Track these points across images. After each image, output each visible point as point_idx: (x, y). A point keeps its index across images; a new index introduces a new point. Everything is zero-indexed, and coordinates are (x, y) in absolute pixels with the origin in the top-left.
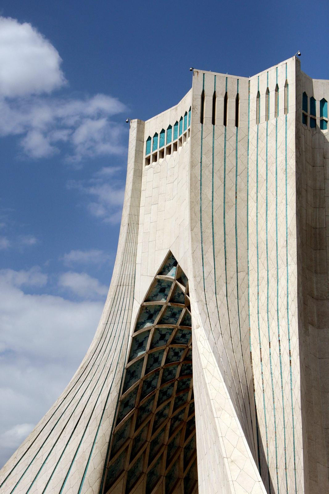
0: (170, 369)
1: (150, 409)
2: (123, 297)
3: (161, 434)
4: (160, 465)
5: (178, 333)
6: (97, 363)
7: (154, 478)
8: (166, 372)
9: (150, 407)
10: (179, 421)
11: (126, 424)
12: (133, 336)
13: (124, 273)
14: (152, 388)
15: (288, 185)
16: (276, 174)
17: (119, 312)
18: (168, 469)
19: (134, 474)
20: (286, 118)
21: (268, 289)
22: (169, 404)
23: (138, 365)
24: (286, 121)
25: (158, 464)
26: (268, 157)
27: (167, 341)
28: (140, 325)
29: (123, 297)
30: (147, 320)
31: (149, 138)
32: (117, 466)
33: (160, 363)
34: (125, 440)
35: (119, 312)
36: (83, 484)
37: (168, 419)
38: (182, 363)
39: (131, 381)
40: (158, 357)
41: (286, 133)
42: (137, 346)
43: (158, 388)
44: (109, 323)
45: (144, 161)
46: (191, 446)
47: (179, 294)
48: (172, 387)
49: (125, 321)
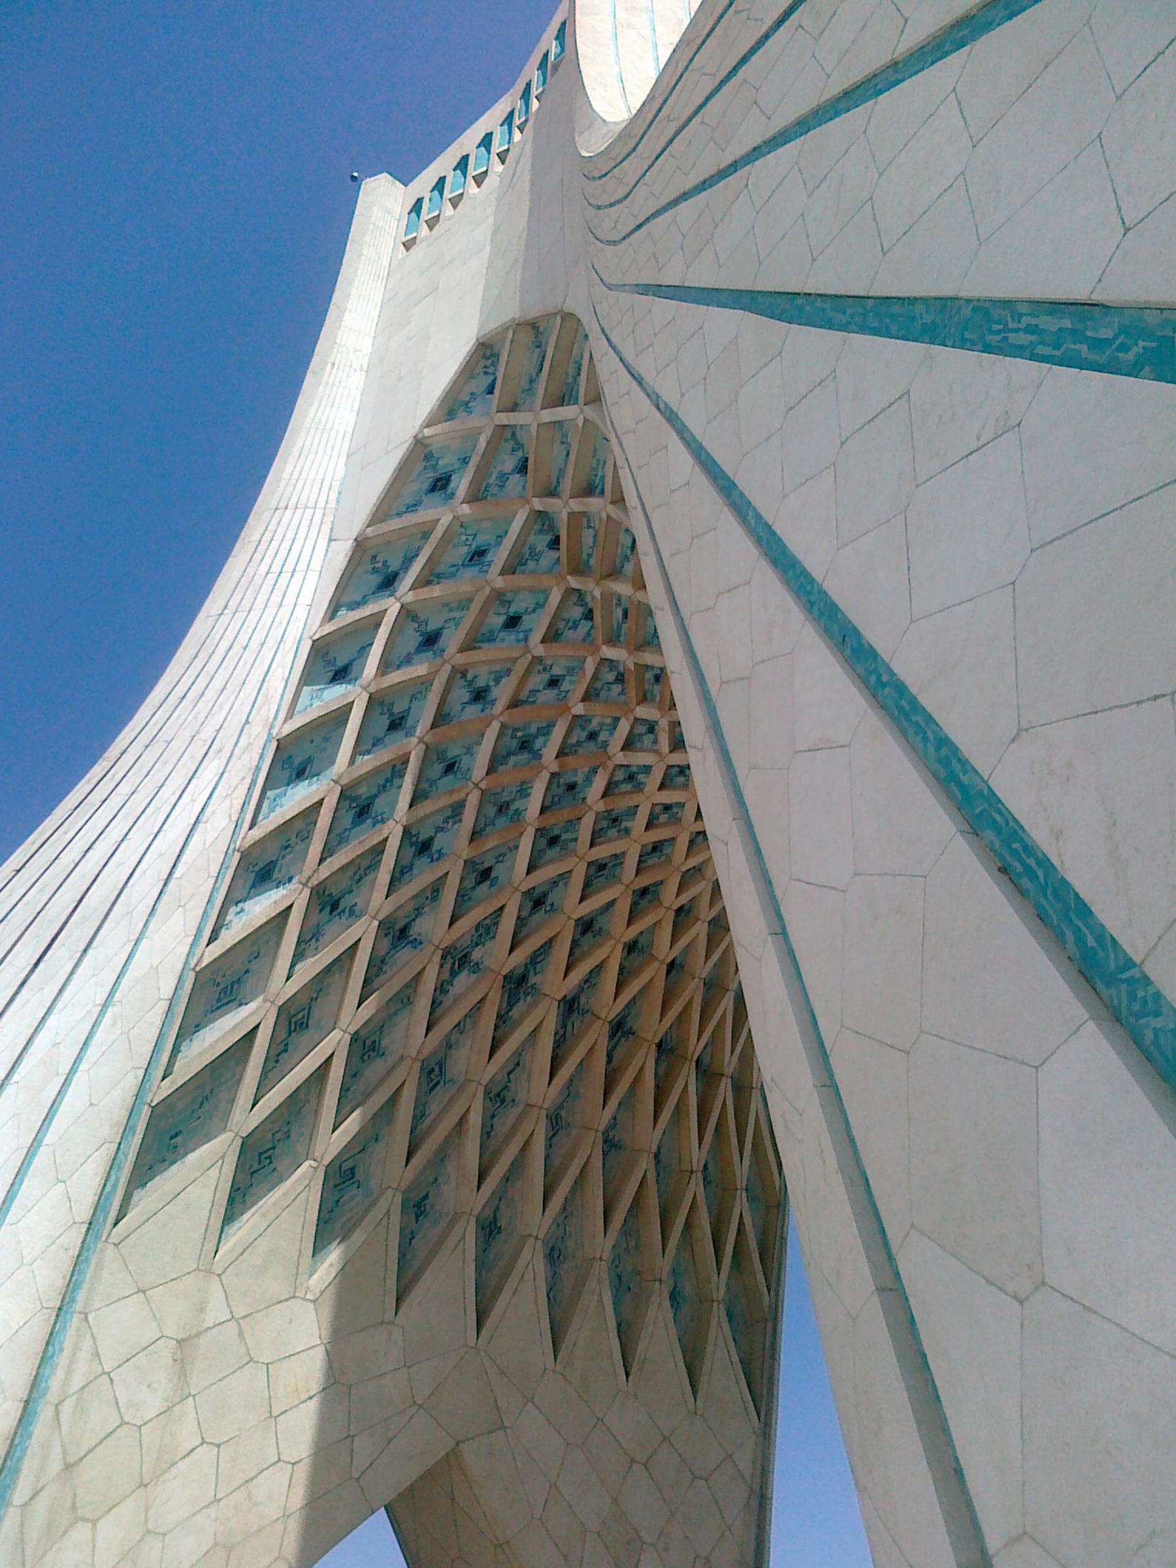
0: (451, 754)
1: (358, 907)
5: (491, 613)
7: (352, 1198)
8: (436, 765)
9: (358, 898)
10: (474, 972)
13: (303, 476)
17: (272, 577)
19: (271, 1163)
22: (436, 890)
23: (326, 739)
25: (377, 1140)
32: (196, 1114)
37: (431, 948)
40: (410, 708)
46: (513, 1089)
48: (454, 823)
49: (289, 600)
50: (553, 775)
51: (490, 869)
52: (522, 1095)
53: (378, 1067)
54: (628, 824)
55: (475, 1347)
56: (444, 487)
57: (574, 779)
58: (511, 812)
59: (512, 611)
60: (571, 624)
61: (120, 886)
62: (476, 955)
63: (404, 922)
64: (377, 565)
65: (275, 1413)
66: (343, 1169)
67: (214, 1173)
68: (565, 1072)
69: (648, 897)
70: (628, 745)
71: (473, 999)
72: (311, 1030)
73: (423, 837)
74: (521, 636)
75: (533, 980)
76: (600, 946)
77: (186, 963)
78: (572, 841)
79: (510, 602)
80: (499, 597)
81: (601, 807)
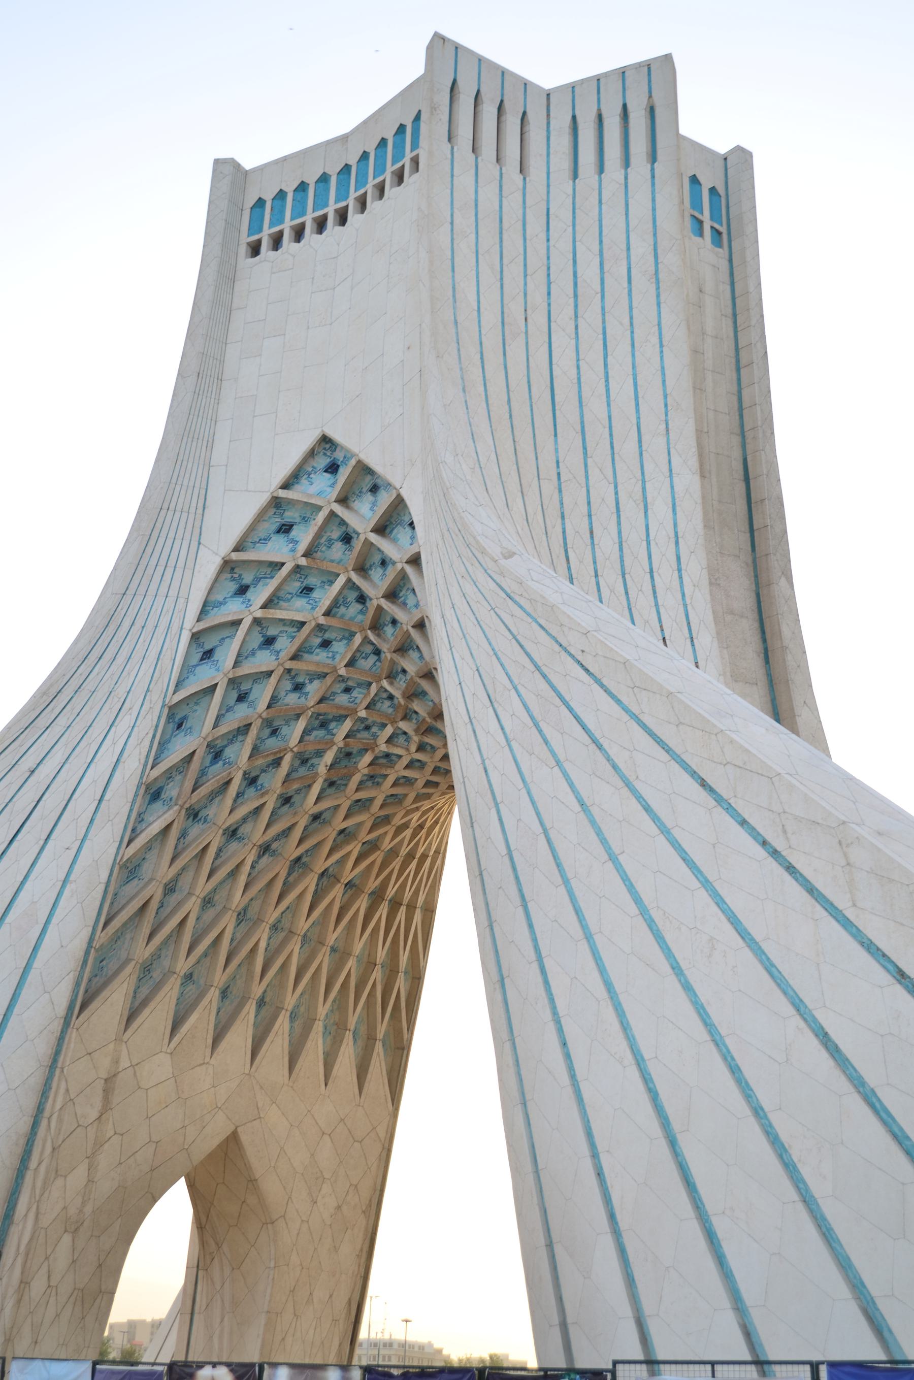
0: (276, 724)
1: (209, 817)
2: (171, 535)
4: (208, 959)
6: (89, 686)
9: (211, 812)
11: (148, 847)
12: (194, 630)
14: (224, 764)
15: (662, 305)
16: (630, 282)
17: (160, 569)
18: (228, 970)
20: (653, 169)
21: (619, 523)
22: (257, 811)
24: (653, 177)
26: (605, 247)
27: (278, 652)
29: (171, 535)
30: (231, 597)
31: (260, 203)
33: (252, 705)
34: (141, 885)
35: (160, 569)
36: (26, 985)
39: (173, 740)
40: (251, 689)
41: (654, 200)
42: (199, 655)
44: (131, 592)
45: (243, 249)
47: (330, 540)
49: (173, 593)
50: (340, 750)
51: (291, 797)
53: (211, 913)
54: (380, 780)
55: (248, 1074)
58: (309, 765)
59: (327, 636)
61: (67, 798)
62: (274, 846)
64: (235, 575)
65: (150, 1115)
67: (125, 985)
68: (316, 913)
70: (389, 741)
71: (271, 876)
72: (176, 893)
73: (253, 774)
74: (330, 655)
75: (304, 859)
76: (348, 844)
77: (115, 860)
80: (320, 628)
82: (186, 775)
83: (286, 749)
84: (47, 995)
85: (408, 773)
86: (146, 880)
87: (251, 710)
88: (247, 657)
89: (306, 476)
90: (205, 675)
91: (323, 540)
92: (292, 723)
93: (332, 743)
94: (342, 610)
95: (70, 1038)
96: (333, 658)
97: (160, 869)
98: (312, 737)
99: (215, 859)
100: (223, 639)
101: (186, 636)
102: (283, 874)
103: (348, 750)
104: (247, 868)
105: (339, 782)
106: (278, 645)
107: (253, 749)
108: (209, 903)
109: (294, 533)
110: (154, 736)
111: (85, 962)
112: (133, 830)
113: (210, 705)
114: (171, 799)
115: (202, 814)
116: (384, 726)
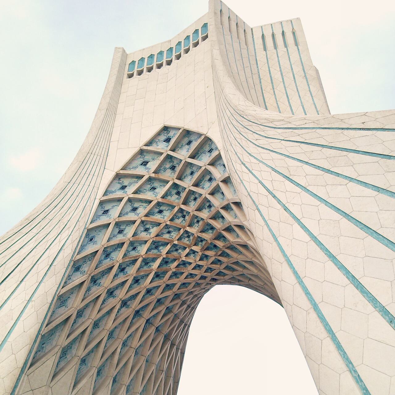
0: (135, 245)
1: (101, 284)
3: (104, 316)
4: (93, 354)
5: (154, 207)
7: (84, 368)
10: (127, 308)
22: (124, 283)
27: (139, 214)
28: (109, 193)
30: (118, 190)
34: (66, 310)
37: (119, 299)
38: (153, 239)
43: (120, 259)
46: (128, 342)
51: (139, 280)
52: (129, 344)
53: (97, 331)
54: (179, 276)
56: (145, 165)
57: (168, 260)
60: (178, 217)
62: (129, 303)
63: (113, 290)
66: (83, 359)
69: (177, 296)
70: (186, 256)
73: (123, 267)
75: (141, 312)
77: (56, 293)
78: (163, 277)
79: (161, 206)
81: (174, 270)
82: (92, 262)
83: (140, 256)
84: (14, 355)
85: (194, 272)
86: (69, 308)
87: (124, 238)
88: (124, 215)
89: (155, 143)
90: (104, 220)
91: (162, 168)
92: (143, 245)
93: (160, 255)
94: (169, 197)
95: (23, 379)
96: (164, 218)
97: (76, 303)
98: (151, 253)
99: (102, 304)
100: (114, 206)
101: (97, 202)
102: (132, 317)
103: (167, 260)
104: (116, 311)
105: (161, 275)
106: (138, 211)
107: (124, 255)
108: (97, 326)
109: (148, 166)
110: (79, 241)
111: (35, 341)
112: (65, 282)
113: (106, 233)
114: (84, 272)
115: (98, 282)
116: (185, 248)
